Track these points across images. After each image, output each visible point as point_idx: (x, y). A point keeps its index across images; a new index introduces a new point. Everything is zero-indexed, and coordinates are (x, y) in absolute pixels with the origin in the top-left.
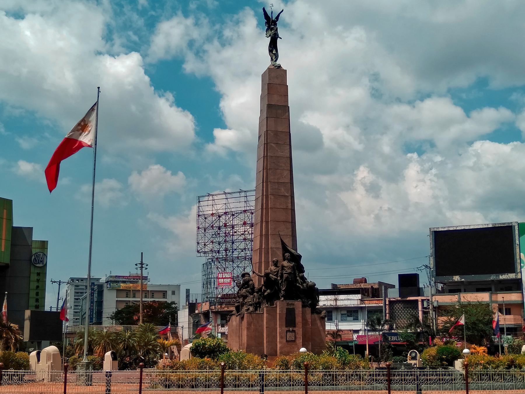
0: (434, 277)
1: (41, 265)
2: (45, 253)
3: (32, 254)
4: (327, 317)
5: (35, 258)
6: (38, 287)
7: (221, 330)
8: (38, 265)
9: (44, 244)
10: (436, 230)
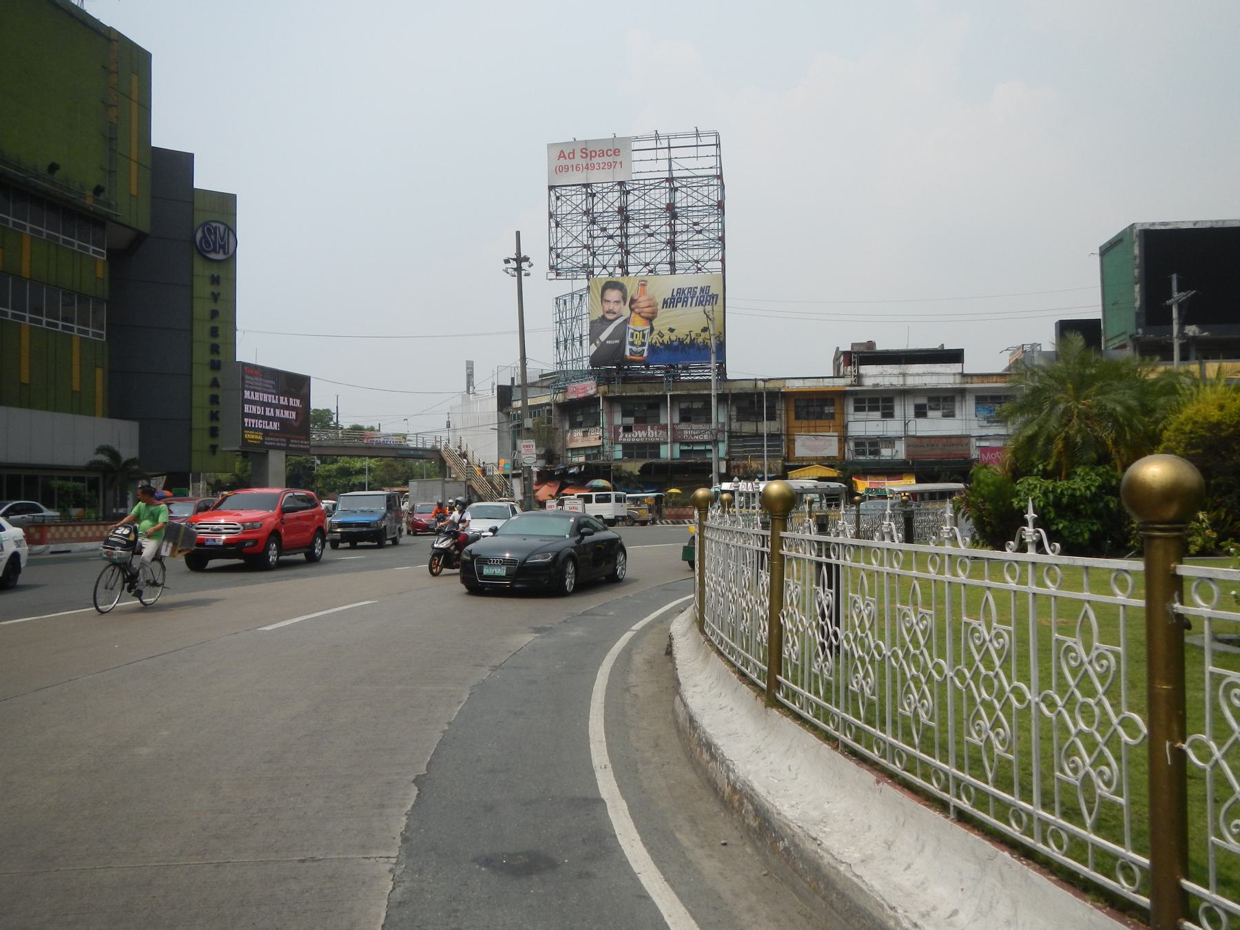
0: (1141, 327)
1: (220, 256)
2: (229, 224)
3: (195, 228)
4: (883, 409)
5: (204, 236)
6: (214, 314)
7: (624, 437)
8: (213, 256)
9: (226, 203)
10: (1147, 227)
